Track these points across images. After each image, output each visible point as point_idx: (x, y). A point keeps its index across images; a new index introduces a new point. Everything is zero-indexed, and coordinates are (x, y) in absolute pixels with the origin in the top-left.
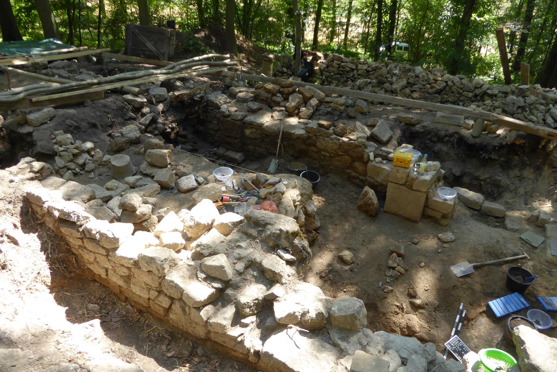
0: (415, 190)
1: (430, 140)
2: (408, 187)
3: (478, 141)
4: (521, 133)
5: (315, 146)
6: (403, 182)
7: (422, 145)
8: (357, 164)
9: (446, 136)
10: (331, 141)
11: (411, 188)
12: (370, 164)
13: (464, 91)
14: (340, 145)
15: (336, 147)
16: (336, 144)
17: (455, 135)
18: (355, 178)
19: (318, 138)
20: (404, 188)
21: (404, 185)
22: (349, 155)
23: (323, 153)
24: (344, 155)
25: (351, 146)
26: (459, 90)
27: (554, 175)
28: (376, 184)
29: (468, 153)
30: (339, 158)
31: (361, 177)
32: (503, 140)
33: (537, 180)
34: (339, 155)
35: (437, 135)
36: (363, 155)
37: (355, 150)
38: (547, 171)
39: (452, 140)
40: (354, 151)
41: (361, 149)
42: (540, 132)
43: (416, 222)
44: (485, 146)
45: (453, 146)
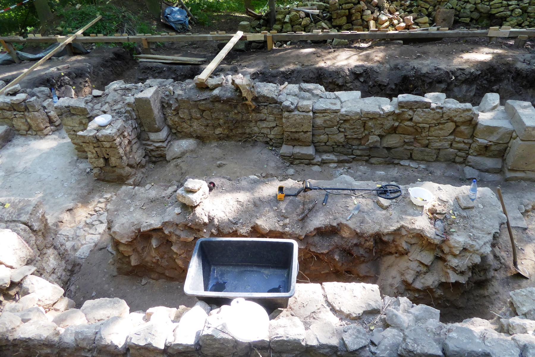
8: (463, 128)
15: (438, 116)
16: (438, 113)
18: (459, 142)
22: (453, 121)
23: (421, 125)
30: (441, 126)
31: (466, 141)
37: (462, 115)
40: (461, 116)
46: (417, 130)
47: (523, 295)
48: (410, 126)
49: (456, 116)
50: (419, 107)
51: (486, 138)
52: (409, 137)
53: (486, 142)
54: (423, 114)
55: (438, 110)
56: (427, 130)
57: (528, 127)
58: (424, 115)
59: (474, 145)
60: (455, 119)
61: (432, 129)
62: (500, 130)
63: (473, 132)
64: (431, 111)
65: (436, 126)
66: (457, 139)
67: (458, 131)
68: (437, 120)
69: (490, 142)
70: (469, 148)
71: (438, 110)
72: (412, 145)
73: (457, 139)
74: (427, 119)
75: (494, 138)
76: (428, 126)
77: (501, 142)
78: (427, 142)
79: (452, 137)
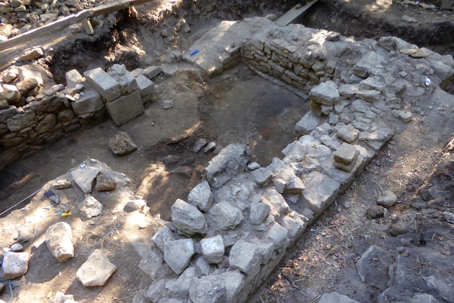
0: (132, 92)
1: (64, 58)
2: (125, 95)
3: (97, 36)
4: (115, 12)
5: (9, 132)
6: (119, 94)
7: (62, 67)
8: (62, 114)
9: (73, 47)
10: (24, 115)
11: (127, 93)
12: (74, 106)
13: (14, 8)
14: (35, 111)
16: (29, 113)
17: (78, 42)
18: (69, 125)
19: (6, 123)
20: (123, 97)
21: (122, 95)
22: (49, 113)
24: (45, 116)
25: (46, 104)
26: (9, 8)
27: (148, 29)
28: (92, 114)
29: (95, 49)
30: (42, 122)
31: (74, 121)
32: (109, 25)
33: (143, 38)
34: (39, 121)
35: (65, 52)
36: (63, 102)
37: (52, 105)
38: (143, 29)
39: (78, 48)
40: (52, 106)
41: (56, 100)
42: (125, 5)
43: (143, 113)
44: (104, 37)
45: (82, 51)
46: (23, 137)
47: (146, 264)
48: (13, 137)
49: (48, 108)
50: (7, 118)
51: (87, 112)
52: (22, 145)
53: (89, 114)
54: (16, 122)
55: (27, 111)
56: (32, 132)
57: (107, 90)
58: (18, 122)
59: (81, 121)
60: (49, 110)
61: (37, 128)
62: (91, 101)
63: (74, 112)
64: (22, 115)
65: (37, 124)
66: (66, 124)
67: (61, 118)
68: (34, 119)
69: (91, 113)
70: (80, 125)
71: (27, 111)
72: (31, 151)
73: (66, 124)
74: (24, 124)
75: (92, 109)
76: (30, 128)
77: (99, 109)
78: (41, 140)
79: (59, 125)
